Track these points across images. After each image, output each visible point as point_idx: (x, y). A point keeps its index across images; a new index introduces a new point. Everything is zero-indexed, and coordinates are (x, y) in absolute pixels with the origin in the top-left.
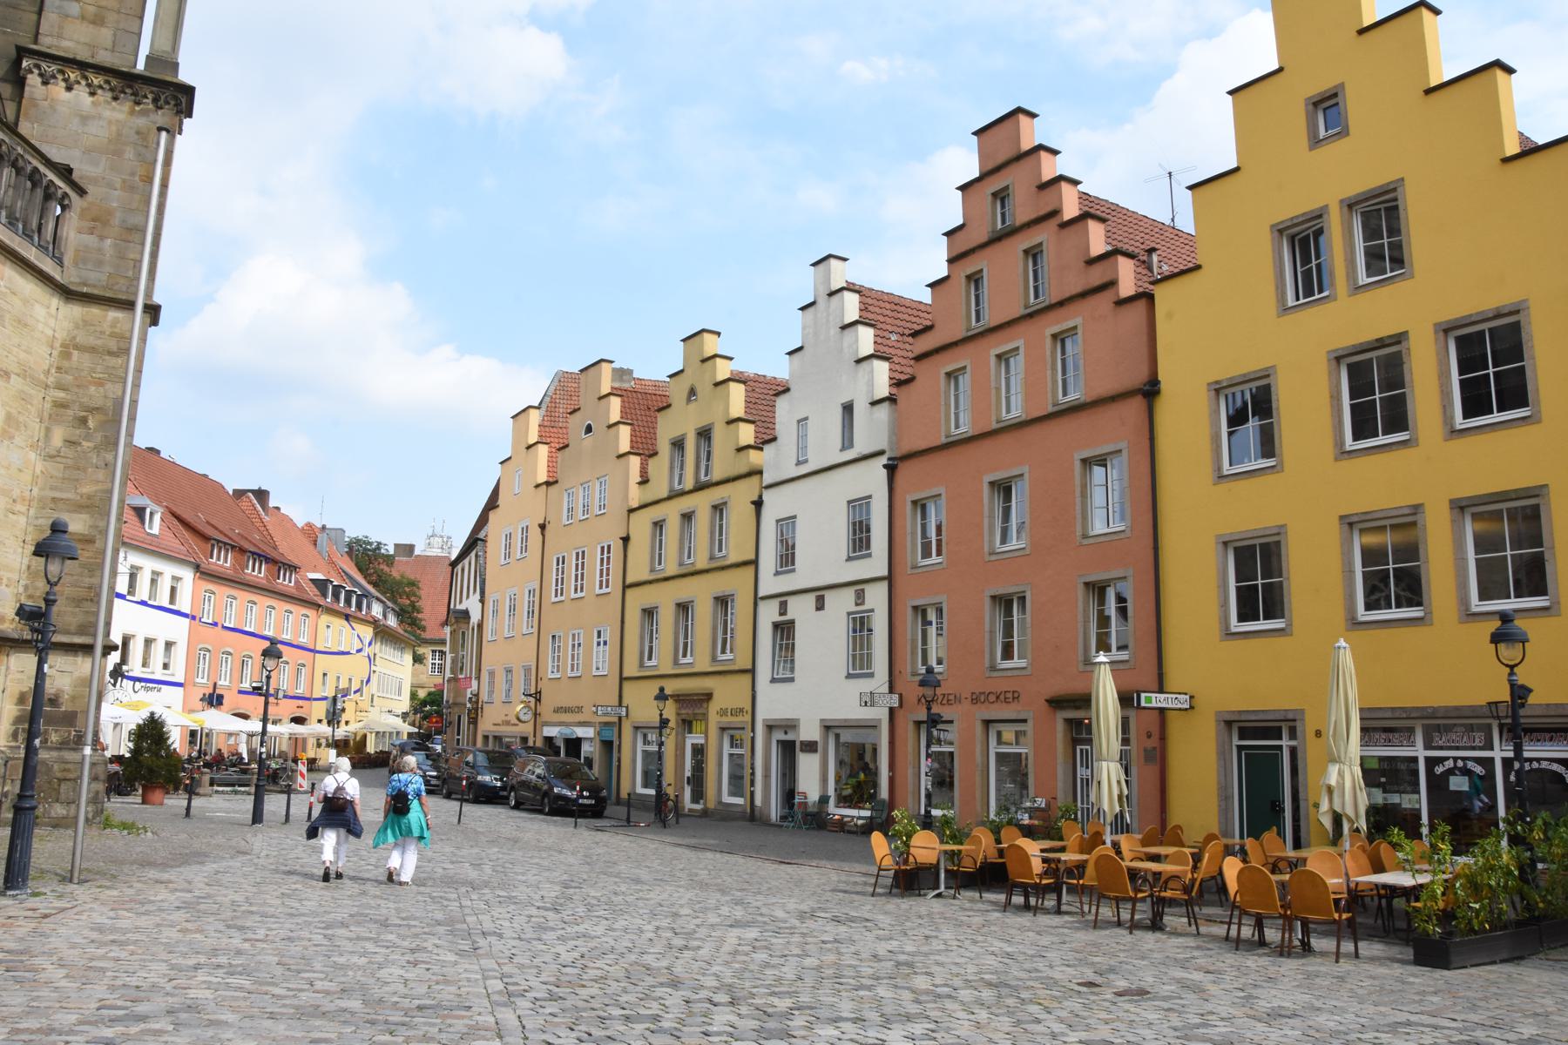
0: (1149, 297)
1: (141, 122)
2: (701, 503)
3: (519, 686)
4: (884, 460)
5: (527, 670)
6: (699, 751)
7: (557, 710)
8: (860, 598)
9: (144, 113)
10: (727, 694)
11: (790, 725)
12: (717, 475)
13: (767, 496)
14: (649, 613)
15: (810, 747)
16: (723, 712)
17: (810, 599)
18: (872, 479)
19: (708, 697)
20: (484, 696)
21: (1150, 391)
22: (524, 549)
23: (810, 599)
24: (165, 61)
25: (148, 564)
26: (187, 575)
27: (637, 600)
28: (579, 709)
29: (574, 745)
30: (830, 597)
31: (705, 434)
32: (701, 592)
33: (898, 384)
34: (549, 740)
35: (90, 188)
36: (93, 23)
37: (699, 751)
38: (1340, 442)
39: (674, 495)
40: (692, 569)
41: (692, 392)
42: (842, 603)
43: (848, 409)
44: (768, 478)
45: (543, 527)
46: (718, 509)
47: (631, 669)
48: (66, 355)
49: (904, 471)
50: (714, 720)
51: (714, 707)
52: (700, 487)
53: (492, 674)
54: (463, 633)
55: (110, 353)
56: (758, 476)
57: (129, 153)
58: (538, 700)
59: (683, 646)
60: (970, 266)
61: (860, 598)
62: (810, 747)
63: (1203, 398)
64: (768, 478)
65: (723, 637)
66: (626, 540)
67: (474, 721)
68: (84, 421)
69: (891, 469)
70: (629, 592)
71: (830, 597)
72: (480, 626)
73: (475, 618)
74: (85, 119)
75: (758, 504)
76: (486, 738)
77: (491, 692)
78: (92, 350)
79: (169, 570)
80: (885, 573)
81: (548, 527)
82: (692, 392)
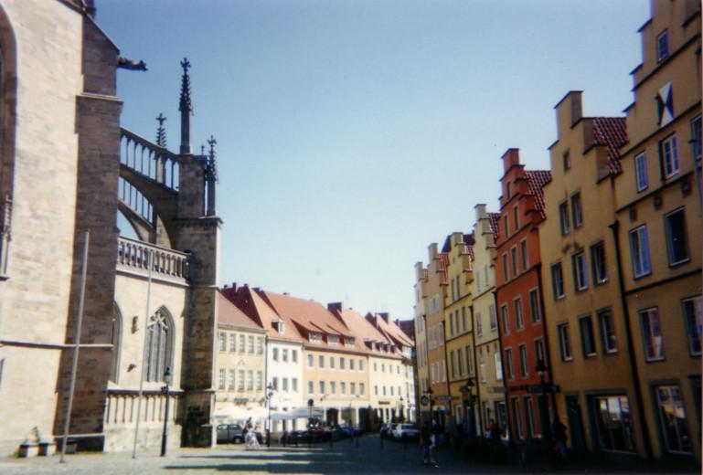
2: (459, 307)
18: (490, 299)
24: (211, 211)
25: (281, 347)
26: (298, 349)
27: (452, 346)
29: (442, 412)
39: (455, 303)
45: (425, 316)
49: (499, 294)
52: (460, 299)
66: (444, 322)
69: (495, 293)
74: (192, 235)
75: (471, 308)
79: (290, 348)
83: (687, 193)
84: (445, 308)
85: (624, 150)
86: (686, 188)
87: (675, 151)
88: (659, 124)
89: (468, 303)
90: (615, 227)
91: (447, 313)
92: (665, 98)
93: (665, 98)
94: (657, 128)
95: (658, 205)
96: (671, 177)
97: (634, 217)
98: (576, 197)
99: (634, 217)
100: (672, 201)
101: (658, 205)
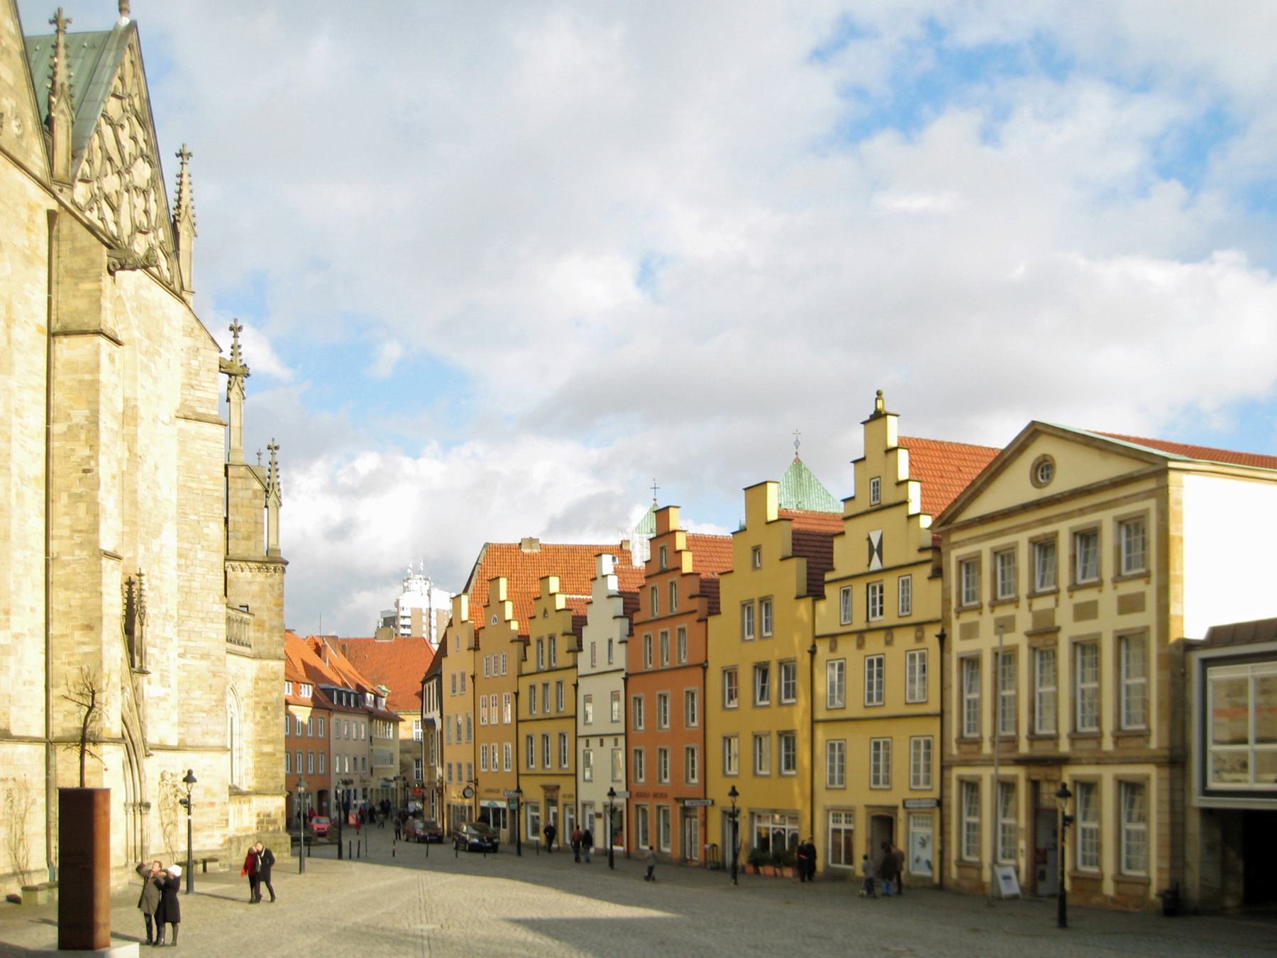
0: (706, 620)
1: (270, 580)
2: (552, 678)
3: (465, 776)
4: (623, 675)
5: (470, 766)
6: (555, 815)
7: (488, 791)
8: (616, 741)
9: (271, 576)
10: (566, 786)
11: (592, 804)
12: (559, 664)
13: (580, 681)
14: (530, 738)
15: (599, 815)
16: (564, 796)
17: (598, 740)
18: (617, 682)
19: (558, 787)
20: (445, 778)
21: (705, 668)
22: (463, 688)
23: (598, 740)
27: (524, 729)
28: (498, 791)
29: (497, 811)
30: (606, 740)
31: (552, 638)
32: (553, 729)
33: (631, 634)
34: (483, 808)
35: (256, 613)
36: (247, 540)
37: (555, 815)
38: (754, 702)
39: (539, 672)
40: (548, 716)
41: (545, 612)
42: (609, 742)
43: (610, 641)
44: (581, 670)
45: (473, 677)
46: (559, 683)
47: (523, 770)
48: (256, 683)
49: (631, 681)
50: (561, 801)
51: (561, 792)
52: (551, 670)
53: (450, 766)
54: (432, 736)
55: (273, 680)
56: (575, 670)
57: (268, 595)
58: (476, 784)
59: (545, 760)
60: (655, 583)
61: (616, 741)
62: (599, 815)
63: (720, 673)
64: (580, 673)
65: (562, 759)
66: (517, 694)
67: (441, 795)
68: (265, 708)
69: (626, 680)
70: (520, 725)
71: (606, 740)
72: (442, 733)
73: (438, 726)
74: (250, 583)
75: (576, 686)
76: (449, 806)
77: (450, 778)
78: (265, 680)
80: (623, 730)
81: (476, 677)
82: (545, 612)
83: (889, 643)
84: (520, 675)
85: (828, 577)
86: (889, 638)
87: (881, 598)
88: (869, 565)
89: (568, 677)
90: (813, 652)
91: (524, 684)
92: (875, 544)
93: (875, 544)
94: (864, 569)
95: (860, 645)
96: (877, 621)
97: (833, 649)
98: (766, 602)
99: (833, 649)
100: (875, 644)
101: (860, 645)
